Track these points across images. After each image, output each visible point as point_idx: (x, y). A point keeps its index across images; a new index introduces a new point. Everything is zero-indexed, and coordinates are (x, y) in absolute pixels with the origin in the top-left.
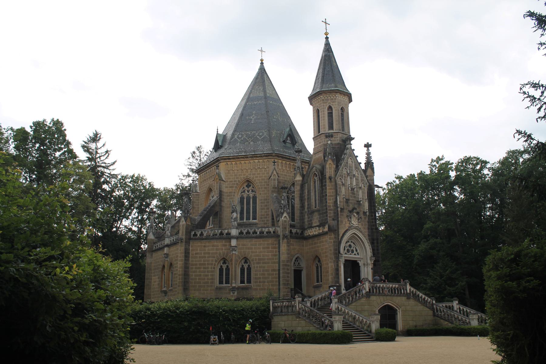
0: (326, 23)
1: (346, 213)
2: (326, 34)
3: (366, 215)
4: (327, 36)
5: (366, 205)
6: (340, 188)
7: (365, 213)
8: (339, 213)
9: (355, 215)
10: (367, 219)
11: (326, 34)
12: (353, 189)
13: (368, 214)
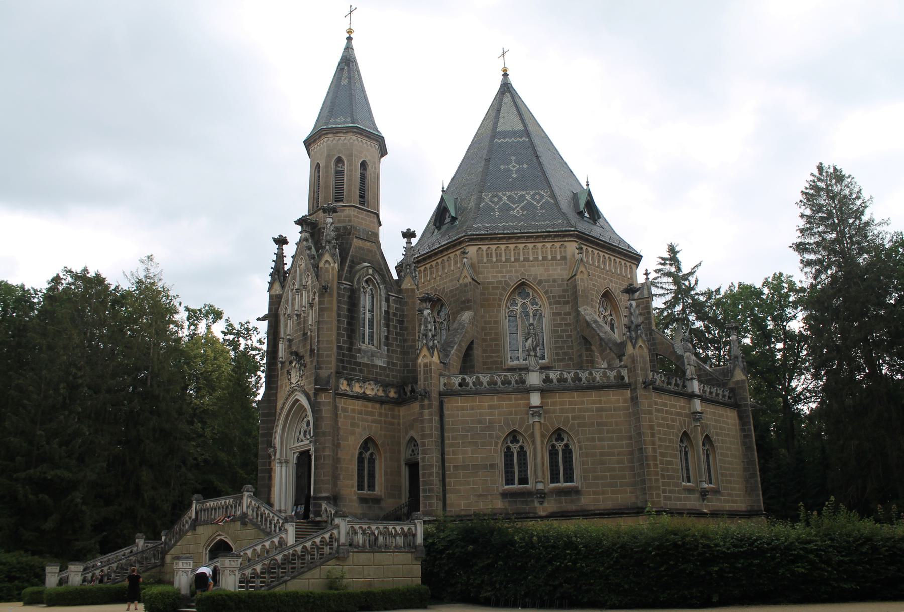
0: (351, 11)
2: (350, 31)
4: (350, 35)
8: (279, 372)
11: (350, 31)
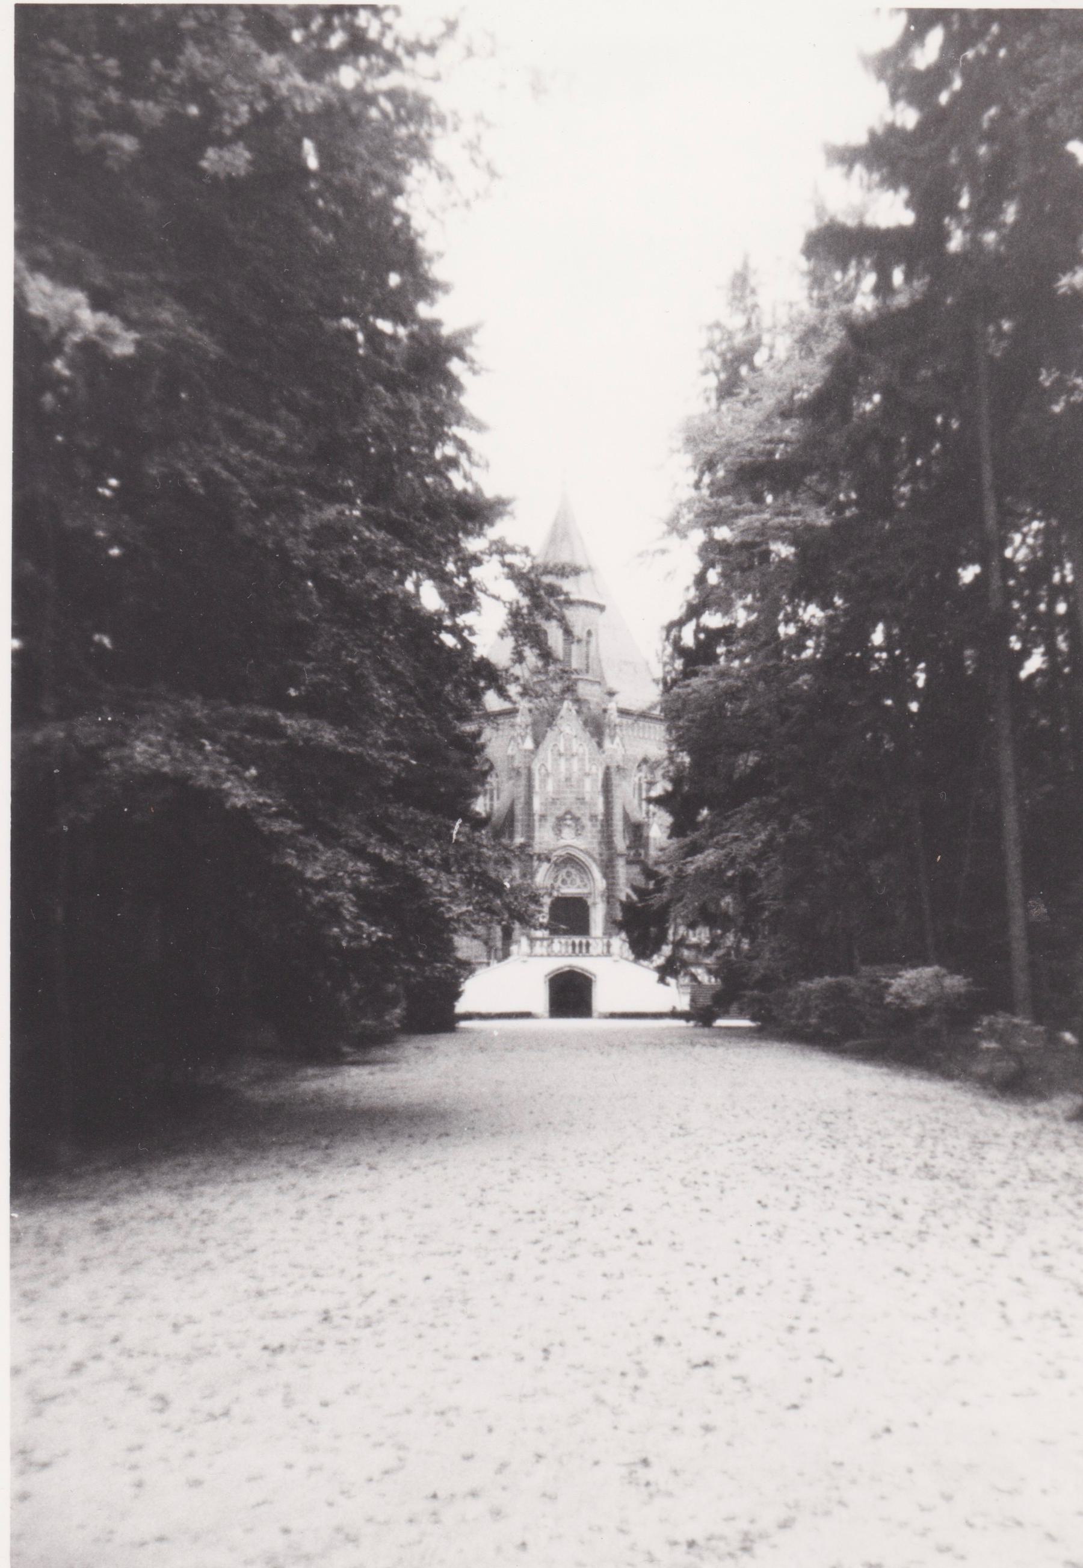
1: (551, 821)
3: (597, 820)
5: (600, 800)
6: (544, 781)
7: (593, 817)
9: (569, 822)
10: (599, 828)
12: (568, 779)
13: (600, 817)
